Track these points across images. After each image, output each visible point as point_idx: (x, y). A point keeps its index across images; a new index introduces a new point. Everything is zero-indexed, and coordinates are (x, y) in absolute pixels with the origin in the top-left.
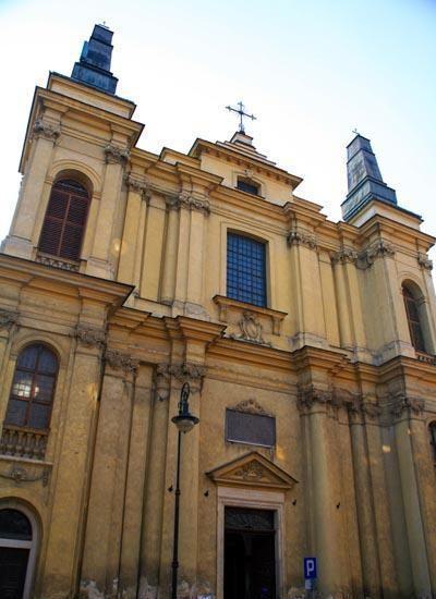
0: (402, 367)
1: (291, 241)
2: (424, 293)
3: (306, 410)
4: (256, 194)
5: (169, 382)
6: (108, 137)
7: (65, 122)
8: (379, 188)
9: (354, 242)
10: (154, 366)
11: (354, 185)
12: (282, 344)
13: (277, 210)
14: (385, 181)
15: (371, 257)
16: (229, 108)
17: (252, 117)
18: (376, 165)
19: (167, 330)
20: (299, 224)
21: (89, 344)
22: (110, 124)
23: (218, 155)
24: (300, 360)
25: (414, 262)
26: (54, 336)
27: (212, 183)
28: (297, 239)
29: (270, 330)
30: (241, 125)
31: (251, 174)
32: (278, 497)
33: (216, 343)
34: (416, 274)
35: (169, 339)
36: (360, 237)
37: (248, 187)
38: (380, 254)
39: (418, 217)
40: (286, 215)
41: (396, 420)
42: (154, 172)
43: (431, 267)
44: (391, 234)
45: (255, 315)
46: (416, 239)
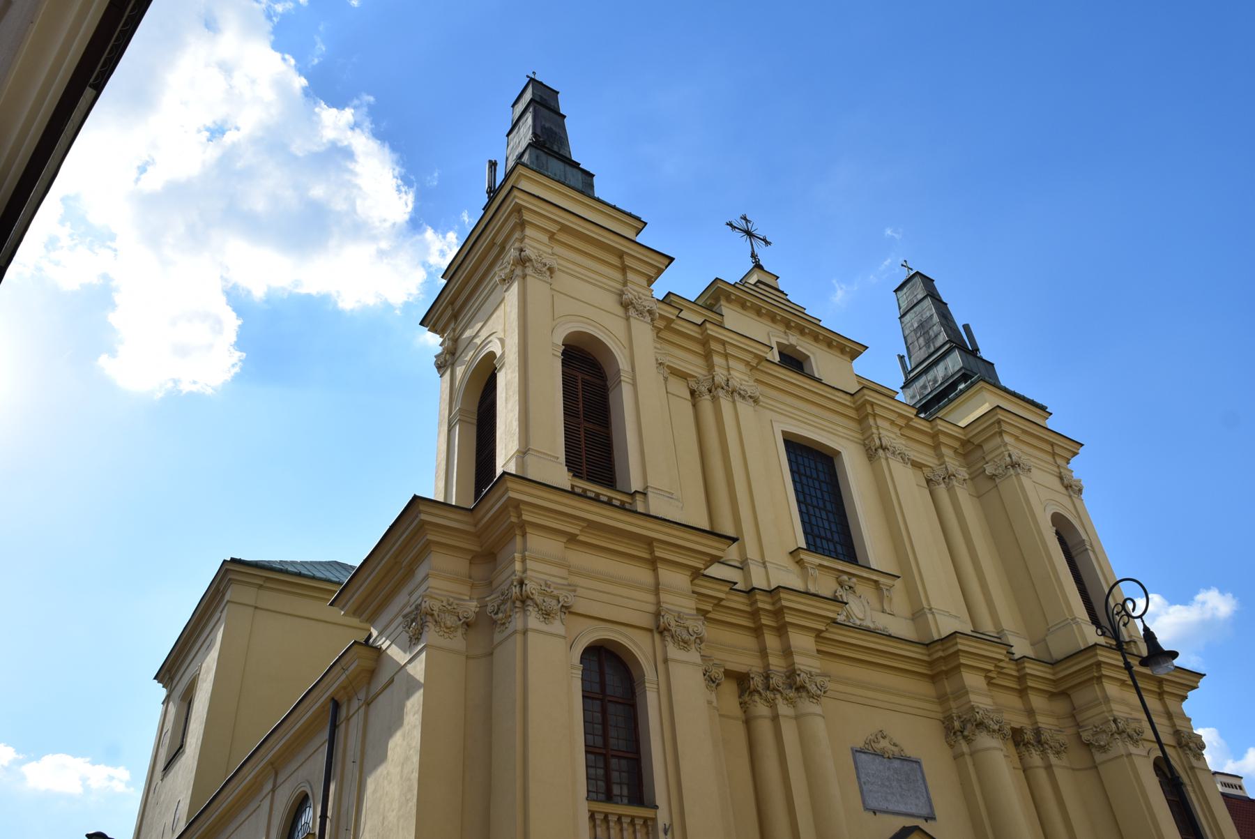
0: (1099, 664)
1: (872, 452)
2: (1084, 537)
3: (964, 747)
5: (773, 706)
6: (618, 275)
9: (956, 451)
10: (741, 680)
11: (922, 354)
13: (848, 397)
14: (985, 354)
15: (992, 477)
16: (730, 224)
17: (767, 243)
19: (755, 614)
20: (879, 422)
21: (684, 644)
22: (621, 254)
23: (743, 305)
24: (939, 660)
27: (756, 356)
28: (884, 449)
29: (878, 606)
30: (753, 255)
31: (794, 339)
34: (1062, 504)
35: (757, 631)
36: (965, 443)
38: (1012, 471)
39: (1043, 408)
40: (857, 410)
41: (1099, 757)
43: (1080, 491)
44: (1017, 438)
45: (854, 580)
46: (1052, 445)
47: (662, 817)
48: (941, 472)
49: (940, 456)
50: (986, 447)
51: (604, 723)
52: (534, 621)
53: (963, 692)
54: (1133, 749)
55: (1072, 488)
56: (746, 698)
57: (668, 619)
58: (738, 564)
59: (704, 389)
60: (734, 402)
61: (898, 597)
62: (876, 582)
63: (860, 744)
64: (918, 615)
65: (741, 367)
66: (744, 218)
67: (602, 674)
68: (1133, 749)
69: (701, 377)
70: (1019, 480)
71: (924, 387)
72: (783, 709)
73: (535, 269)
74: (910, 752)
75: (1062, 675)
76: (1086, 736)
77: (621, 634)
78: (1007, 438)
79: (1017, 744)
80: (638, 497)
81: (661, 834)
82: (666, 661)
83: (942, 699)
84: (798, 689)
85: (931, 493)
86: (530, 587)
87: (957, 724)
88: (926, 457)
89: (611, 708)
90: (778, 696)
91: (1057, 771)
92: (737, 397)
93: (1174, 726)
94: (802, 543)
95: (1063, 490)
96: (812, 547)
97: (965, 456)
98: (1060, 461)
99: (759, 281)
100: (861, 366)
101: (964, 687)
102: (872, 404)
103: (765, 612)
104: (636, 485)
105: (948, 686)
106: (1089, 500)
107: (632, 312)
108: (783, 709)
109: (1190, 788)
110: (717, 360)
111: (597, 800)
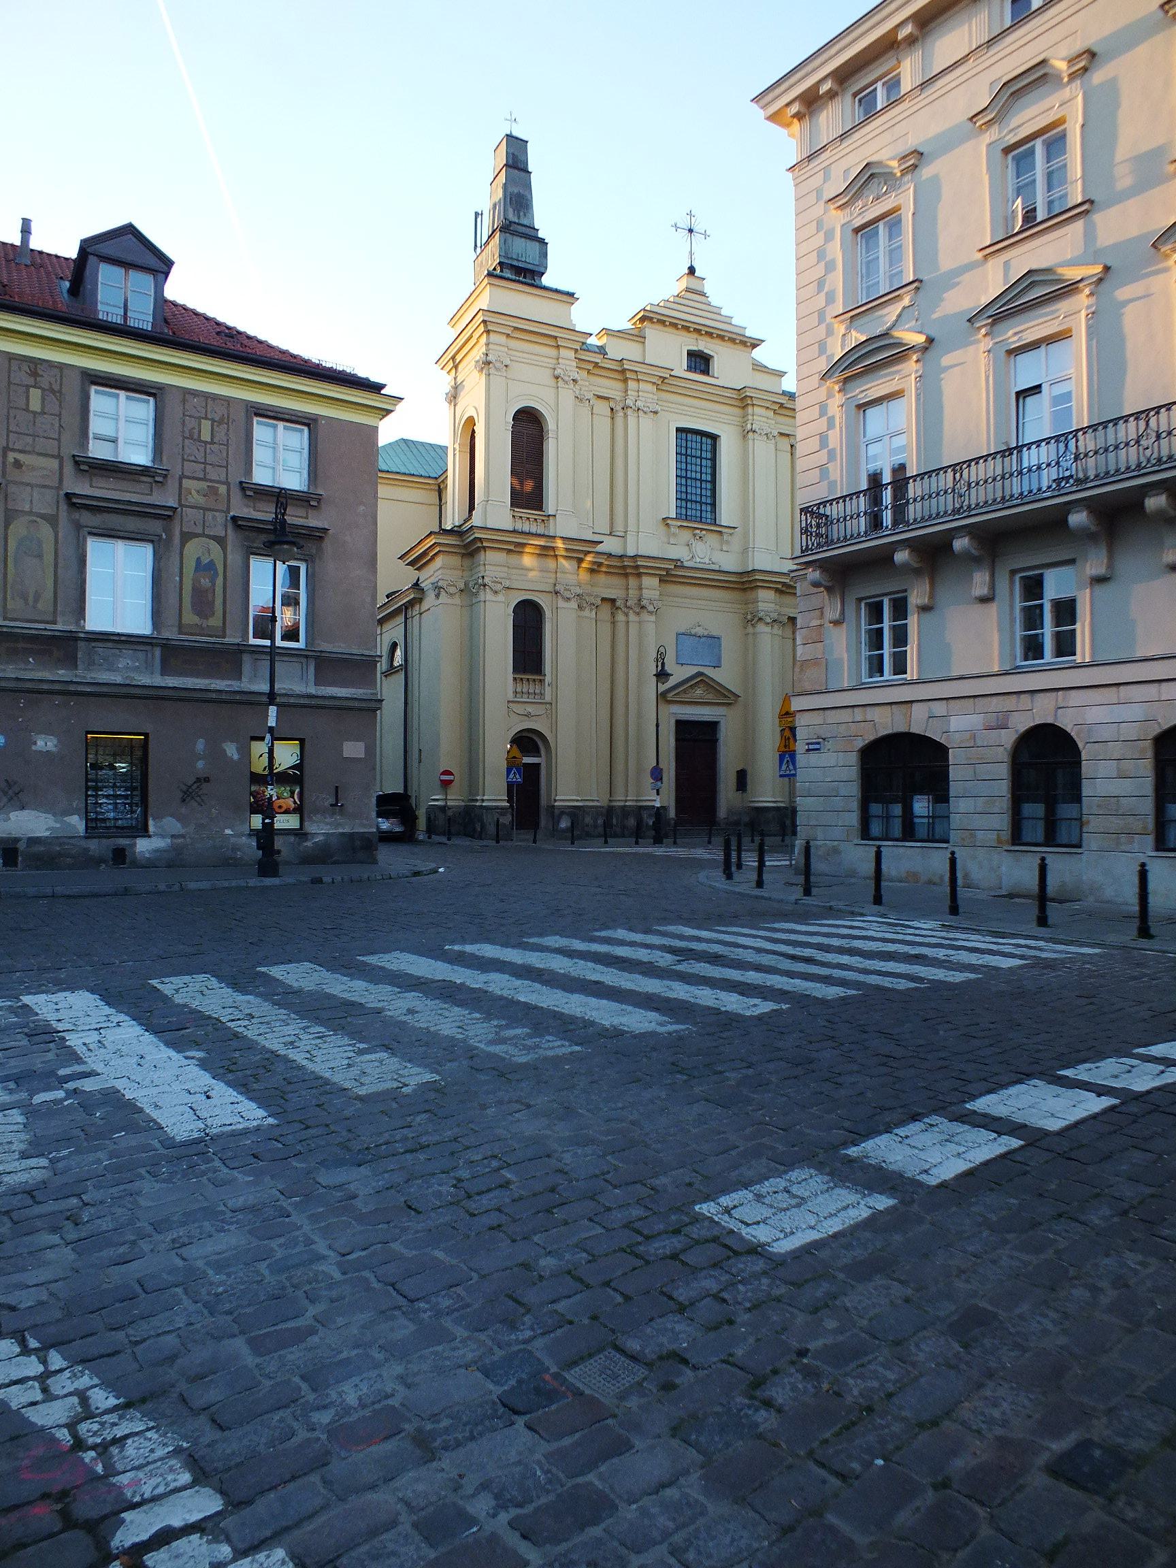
1: (746, 433)
3: (750, 630)
4: (706, 372)
5: (627, 615)
6: (553, 352)
7: (513, 343)
10: (613, 601)
12: (729, 561)
16: (676, 227)
24: (745, 583)
32: (721, 710)
33: (672, 574)
35: (626, 575)
37: (700, 362)
42: (597, 371)
47: (548, 679)
52: (489, 596)
58: (622, 534)
59: (619, 408)
61: (736, 542)
63: (683, 631)
64: (745, 551)
65: (650, 387)
66: (690, 214)
69: (618, 398)
72: (632, 617)
73: (497, 369)
74: (714, 633)
86: (487, 580)
87: (749, 617)
92: (641, 413)
99: (688, 290)
100: (757, 354)
103: (628, 567)
107: (561, 383)
108: (632, 617)
110: (632, 384)
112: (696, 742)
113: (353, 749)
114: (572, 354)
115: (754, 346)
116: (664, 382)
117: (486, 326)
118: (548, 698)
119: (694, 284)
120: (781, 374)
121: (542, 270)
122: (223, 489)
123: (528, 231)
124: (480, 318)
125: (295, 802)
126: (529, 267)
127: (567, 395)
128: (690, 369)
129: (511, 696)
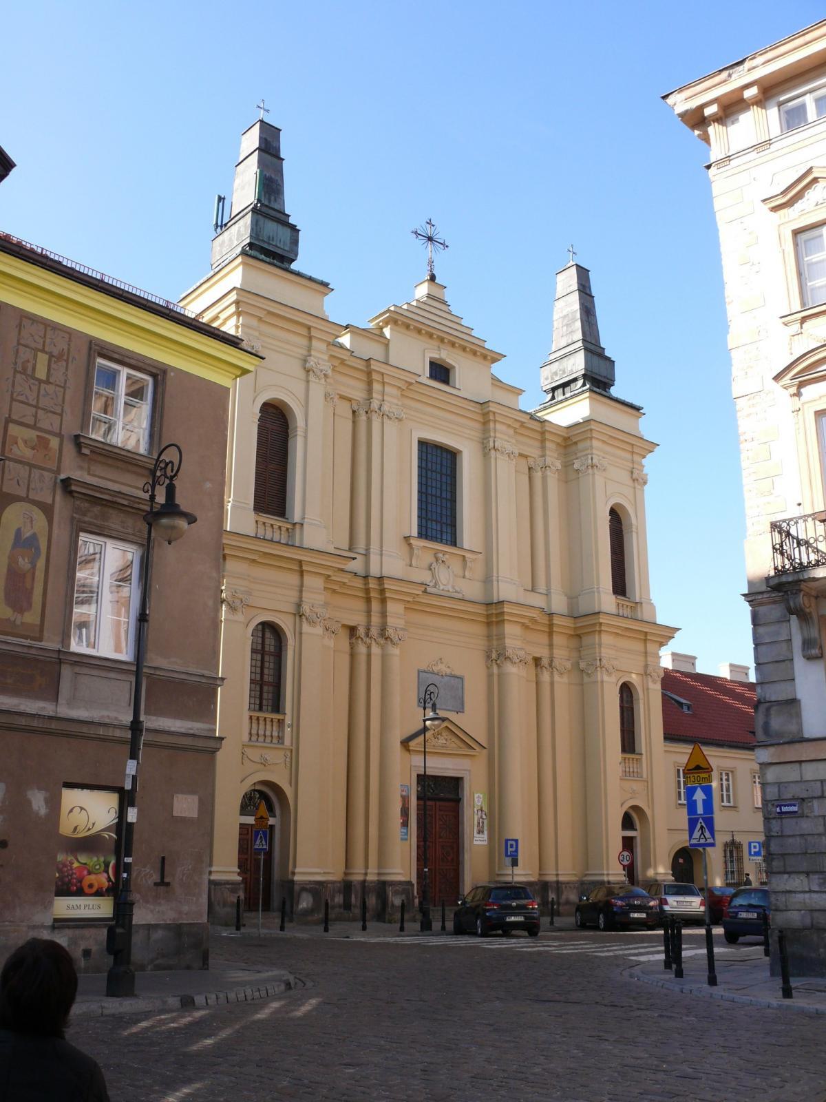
1: (486, 450)
2: (634, 521)
5: (369, 647)
6: (304, 342)
7: (265, 328)
8: (596, 360)
9: (558, 444)
12: (472, 590)
13: (478, 406)
14: (607, 353)
16: (416, 233)
17: (445, 246)
18: (594, 316)
19: (367, 591)
20: (498, 426)
25: (624, 476)
26: (278, 615)
27: (406, 382)
29: (461, 573)
36: (566, 439)
37: (441, 372)
38: (590, 471)
39: (638, 409)
41: (586, 679)
43: (645, 483)
44: (604, 442)
46: (633, 445)
47: (288, 721)
48: (540, 461)
49: (543, 448)
50: (581, 446)
51: (262, 667)
53: (501, 637)
54: (606, 678)
55: (638, 480)
56: (354, 640)
57: (306, 608)
60: (383, 423)
62: (464, 556)
63: (424, 668)
64: (488, 580)
65: (395, 391)
67: (263, 638)
68: (606, 678)
70: (594, 478)
71: (556, 373)
72: (375, 650)
75: (578, 625)
76: (582, 665)
77: (274, 616)
78: (595, 443)
79: (536, 665)
80: (298, 527)
81: (286, 727)
82: (301, 633)
83: (489, 637)
84: (386, 639)
85: (530, 478)
87: (494, 656)
88: (533, 451)
89: (267, 658)
90: (373, 642)
91: (556, 686)
93: (646, 661)
94: (415, 532)
95: (630, 482)
96: (424, 534)
97: (565, 447)
98: (636, 458)
100: (497, 369)
101: (504, 634)
102: (494, 413)
104: (297, 519)
105: (494, 630)
106: (650, 493)
109: (641, 702)
111: (254, 710)
112: (439, 799)
113: (185, 806)
114: (323, 346)
115: (494, 360)
116: (408, 387)
117: (237, 308)
118: (287, 741)
119: (436, 292)
120: (518, 392)
121: (292, 256)
122: (54, 442)
123: (278, 215)
124: (233, 297)
125: (109, 880)
126: (279, 252)
127: (318, 390)
128: (433, 376)
129: (246, 737)
